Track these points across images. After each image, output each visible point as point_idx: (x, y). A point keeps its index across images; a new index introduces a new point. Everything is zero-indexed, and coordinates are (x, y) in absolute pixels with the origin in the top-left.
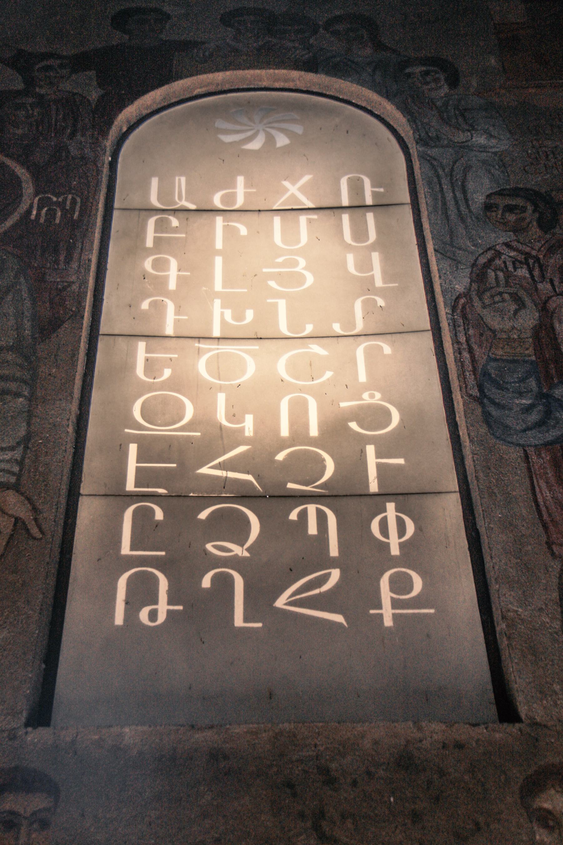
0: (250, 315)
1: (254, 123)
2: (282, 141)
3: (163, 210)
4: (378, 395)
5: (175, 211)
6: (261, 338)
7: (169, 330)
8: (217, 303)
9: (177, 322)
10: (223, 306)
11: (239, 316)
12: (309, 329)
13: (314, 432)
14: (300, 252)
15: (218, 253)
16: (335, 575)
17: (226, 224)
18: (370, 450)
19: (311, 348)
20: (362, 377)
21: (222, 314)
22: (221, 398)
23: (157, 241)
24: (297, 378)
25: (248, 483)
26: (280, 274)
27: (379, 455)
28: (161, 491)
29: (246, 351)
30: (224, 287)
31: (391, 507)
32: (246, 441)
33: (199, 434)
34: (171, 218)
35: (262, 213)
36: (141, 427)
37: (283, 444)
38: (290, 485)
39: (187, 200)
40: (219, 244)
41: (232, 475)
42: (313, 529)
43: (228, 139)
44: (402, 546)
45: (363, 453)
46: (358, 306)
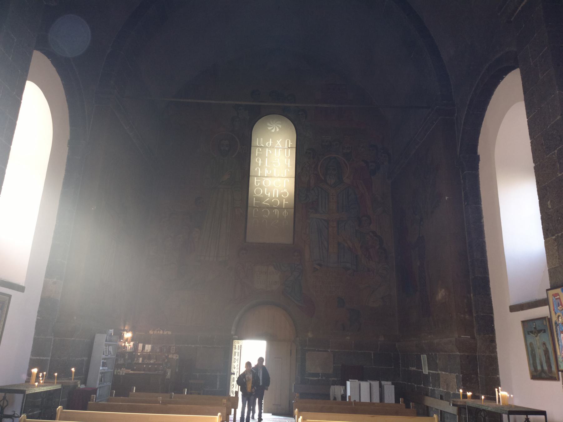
0: (270, 171)
2: (278, 130)
3: (259, 147)
4: (286, 190)
7: (259, 175)
10: (267, 170)
11: (269, 172)
13: (277, 196)
18: (284, 200)
20: (285, 187)
23: (258, 154)
28: (258, 206)
31: (285, 210)
32: (269, 198)
37: (274, 198)
40: (267, 156)
42: (276, 214)
43: (269, 128)
46: (286, 170)
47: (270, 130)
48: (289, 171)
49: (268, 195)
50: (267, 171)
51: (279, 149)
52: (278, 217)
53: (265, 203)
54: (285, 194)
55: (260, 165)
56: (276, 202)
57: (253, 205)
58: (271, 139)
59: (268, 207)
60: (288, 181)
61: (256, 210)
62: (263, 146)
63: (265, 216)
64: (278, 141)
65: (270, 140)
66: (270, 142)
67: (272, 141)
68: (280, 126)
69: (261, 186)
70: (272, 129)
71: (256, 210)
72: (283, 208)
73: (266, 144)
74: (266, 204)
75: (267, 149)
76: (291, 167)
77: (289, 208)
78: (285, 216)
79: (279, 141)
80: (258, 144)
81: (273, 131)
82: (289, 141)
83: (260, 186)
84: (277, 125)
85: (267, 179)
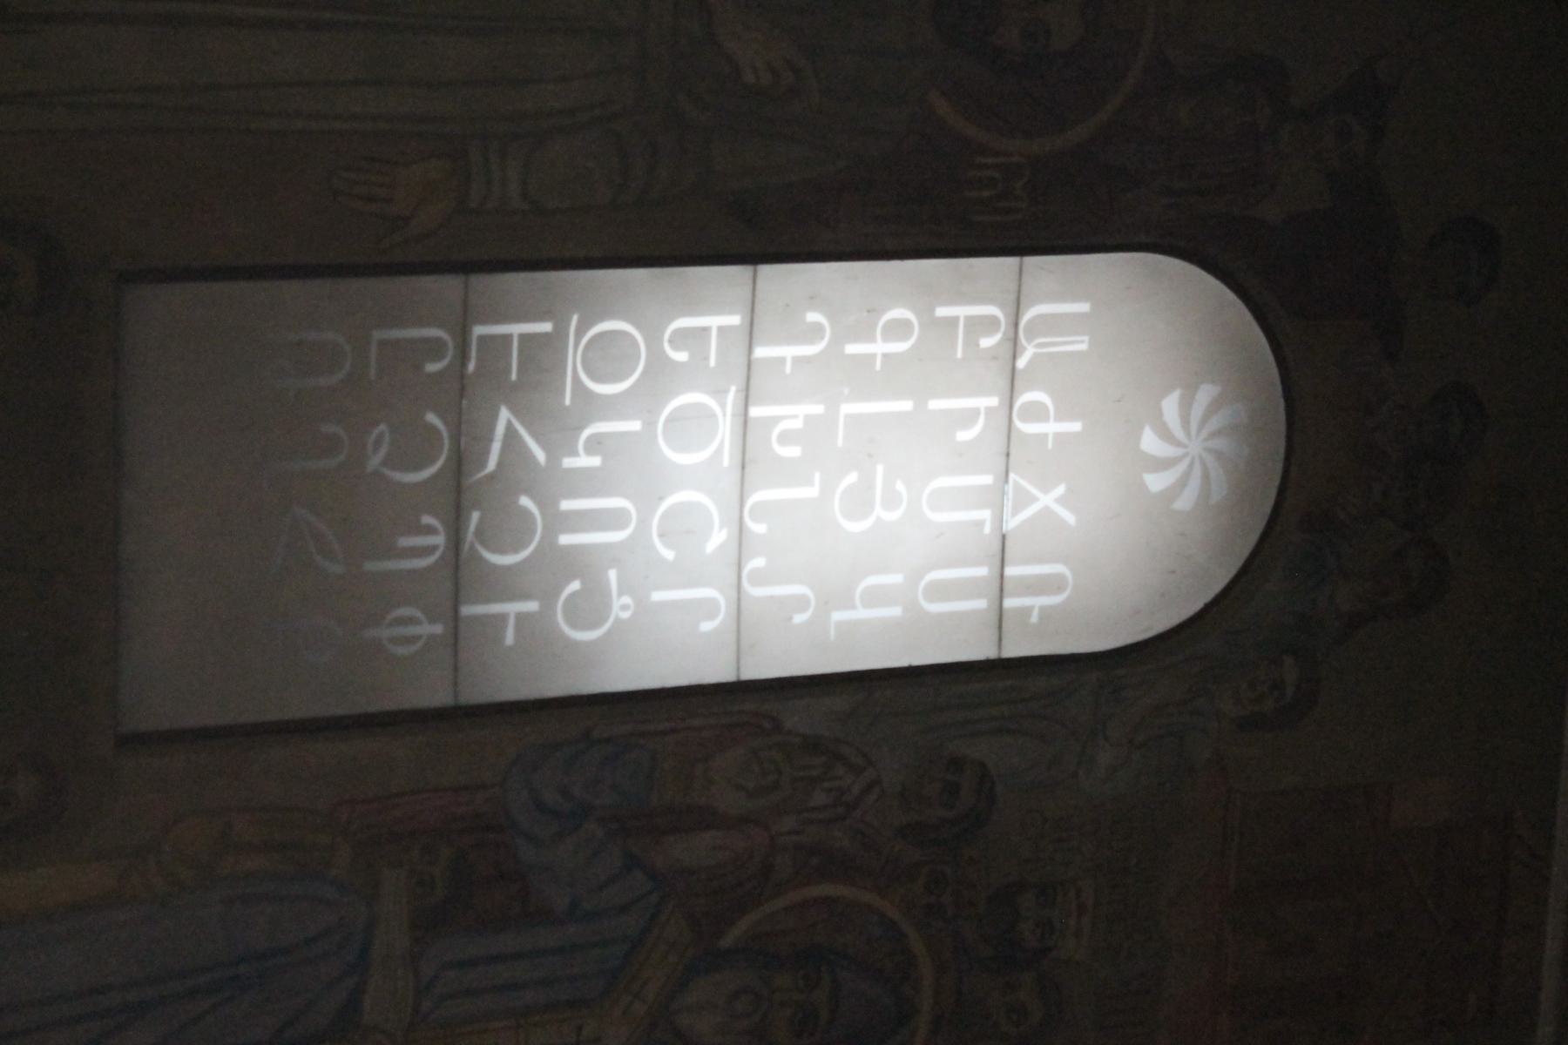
0: (793, 451)
1: (1206, 440)
2: (1156, 482)
3: (1016, 325)
4: (625, 615)
5: (1015, 341)
6: (743, 467)
7: (760, 352)
8: (818, 409)
9: (781, 361)
10: (808, 419)
11: (785, 438)
12: (757, 528)
13: (565, 539)
16: (336, 569)
17: (982, 411)
18: (531, 606)
19: (721, 528)
20: (658, 596)
21: (795, 417)
22: (634, 426)
23: (953, 322)
24: (665, 516)
25: (483, 463)
27: (522, 618)
28: (471, 367)
29: (719, 451)
30: (848, 417)
31: (438, 629)
32: (553, 458)
33: (568, 402)
34: (997, 337)
35: (1003, 459)
36: (580, 333)
37: (547, 504)
38: (475, 516)
39: (1036, 356)
40: (935, 404)
43: (1170, 406)
44: (432, 621)
45: (526, 597)
47: (1160, 414)
49: (575, 453)
50: (798, 424)
51: (986, 515)
52: (371, 566)
53: (500, 429)
54: (590, 608)
56: (515, 530)
57: (485, 321)
58: (1075, 426)
59: (460, 464)
60: (707, 626)
61: (434, 349)
62: (1021, 363)
63: (378, 443)
64: (1060, 490)
66: (1059, 418)
68: (1185, 502)
70: (1165, 434)
71: (434, 349)
72: (456, 610)
74: (491, 440)
75: (993, 401)
76: (832, 632)
77: (456, 669)
78: (385, 633)
79: (1061, 501)
80: (1042, 318)
81: (1150, 442)
82: (1060, 589)
83: (658, 363)
84: (1197, 472)
85: (726, 428)
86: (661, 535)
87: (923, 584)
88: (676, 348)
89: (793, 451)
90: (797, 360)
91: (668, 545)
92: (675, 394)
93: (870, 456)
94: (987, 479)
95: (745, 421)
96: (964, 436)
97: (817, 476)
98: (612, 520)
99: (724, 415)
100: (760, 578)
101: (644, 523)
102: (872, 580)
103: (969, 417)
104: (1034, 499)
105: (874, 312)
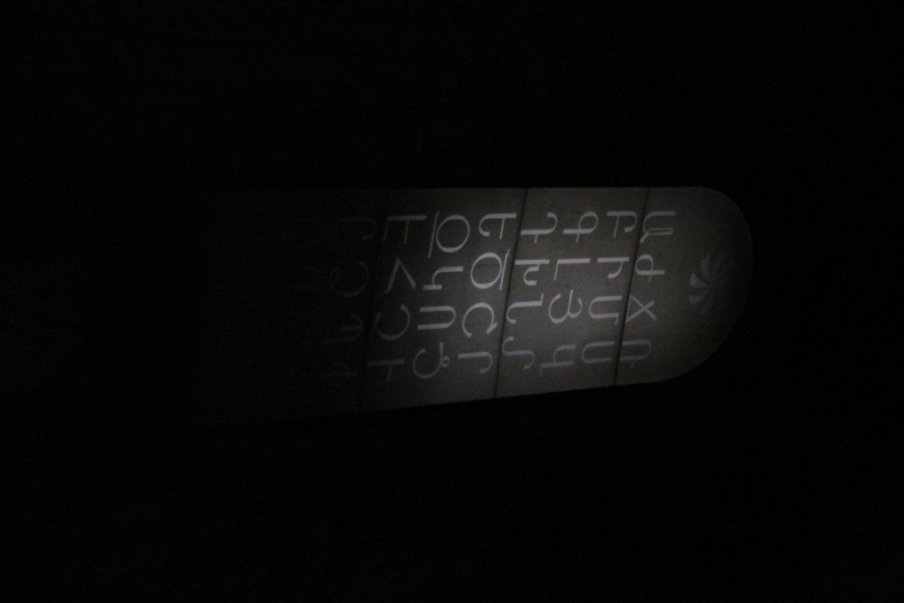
0: (532, 283)
2: (694, 300)
4: (445, 366)
9: (533, 236)
10: (542, 267)
11: (531, 276)
13: (421, 327)
14: (585, 314)
15: (594, 260)
18: (401, 361)
19: (494, 322)
20: (462, 356)
21: (535, 265)
22: (460, 269)
23: (613, 219)
26: (567, 301)
28: (385, 237)
29: (497, 284)
30: (560, 265)
32: (419, 284)
38: (379, 315)
40: (601, 260)
41: (392, 279)
43: (705, 264)
48: (526, 367)
49: (431, 284)
50: (536, 269)
51: (616, 315)
53: (395, 270)
55: (567, 231)
58: (662, 272)
62: (642, 240)
64: (651, 303)
65: (659, 269)
67: (655, 277)
69: (476, 245)
70: (700, 276)
73: (650, 254)
75: (627, 259)
80: (652, 218)
81: (694, 281)
83: (475, 235)
85: (502, 271)
86: (466, 325)
87: (585, 349)
88: (484, 229)
89: (532, 283)
90: (541, 237)
91: (469, 330)
92: (481, 253)
93: (568, 286)
94: (618, 298)
95: (512, 267)
96: (612, 276)
97: (542, 296)
98: (444, 317)
99: (503, 264)
100: (511, 346)
101: (459, 319)
102: (562, 348)
103: (613, 267)
104: (638, 308)
105: (580, 213)
